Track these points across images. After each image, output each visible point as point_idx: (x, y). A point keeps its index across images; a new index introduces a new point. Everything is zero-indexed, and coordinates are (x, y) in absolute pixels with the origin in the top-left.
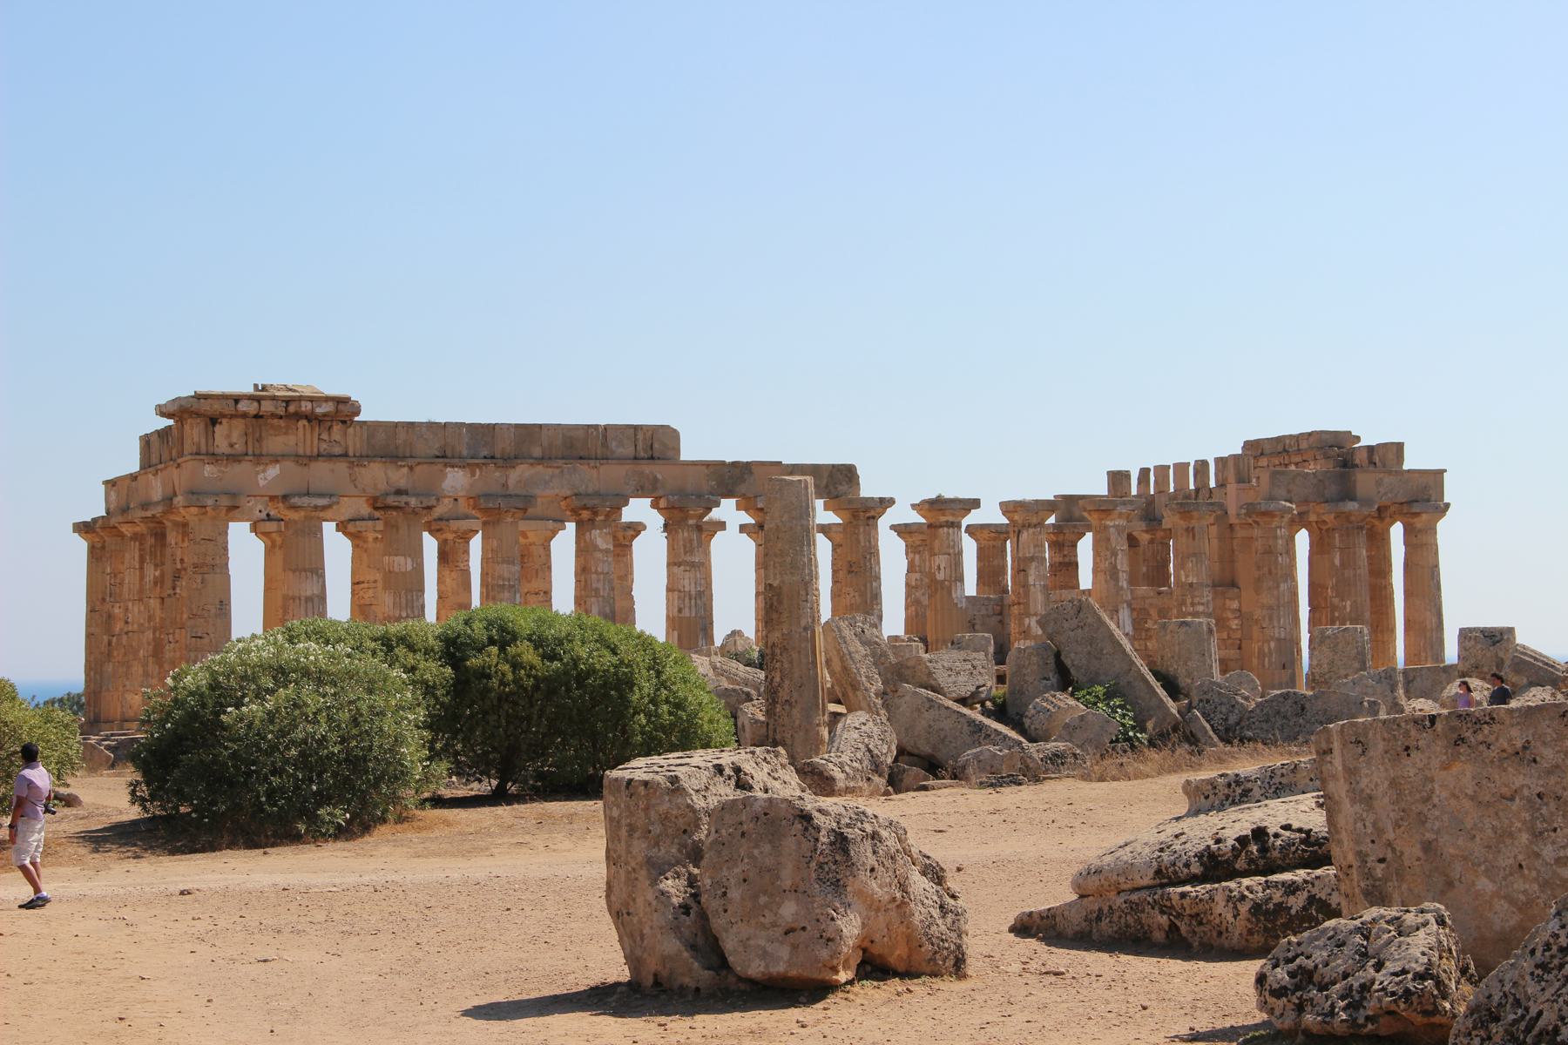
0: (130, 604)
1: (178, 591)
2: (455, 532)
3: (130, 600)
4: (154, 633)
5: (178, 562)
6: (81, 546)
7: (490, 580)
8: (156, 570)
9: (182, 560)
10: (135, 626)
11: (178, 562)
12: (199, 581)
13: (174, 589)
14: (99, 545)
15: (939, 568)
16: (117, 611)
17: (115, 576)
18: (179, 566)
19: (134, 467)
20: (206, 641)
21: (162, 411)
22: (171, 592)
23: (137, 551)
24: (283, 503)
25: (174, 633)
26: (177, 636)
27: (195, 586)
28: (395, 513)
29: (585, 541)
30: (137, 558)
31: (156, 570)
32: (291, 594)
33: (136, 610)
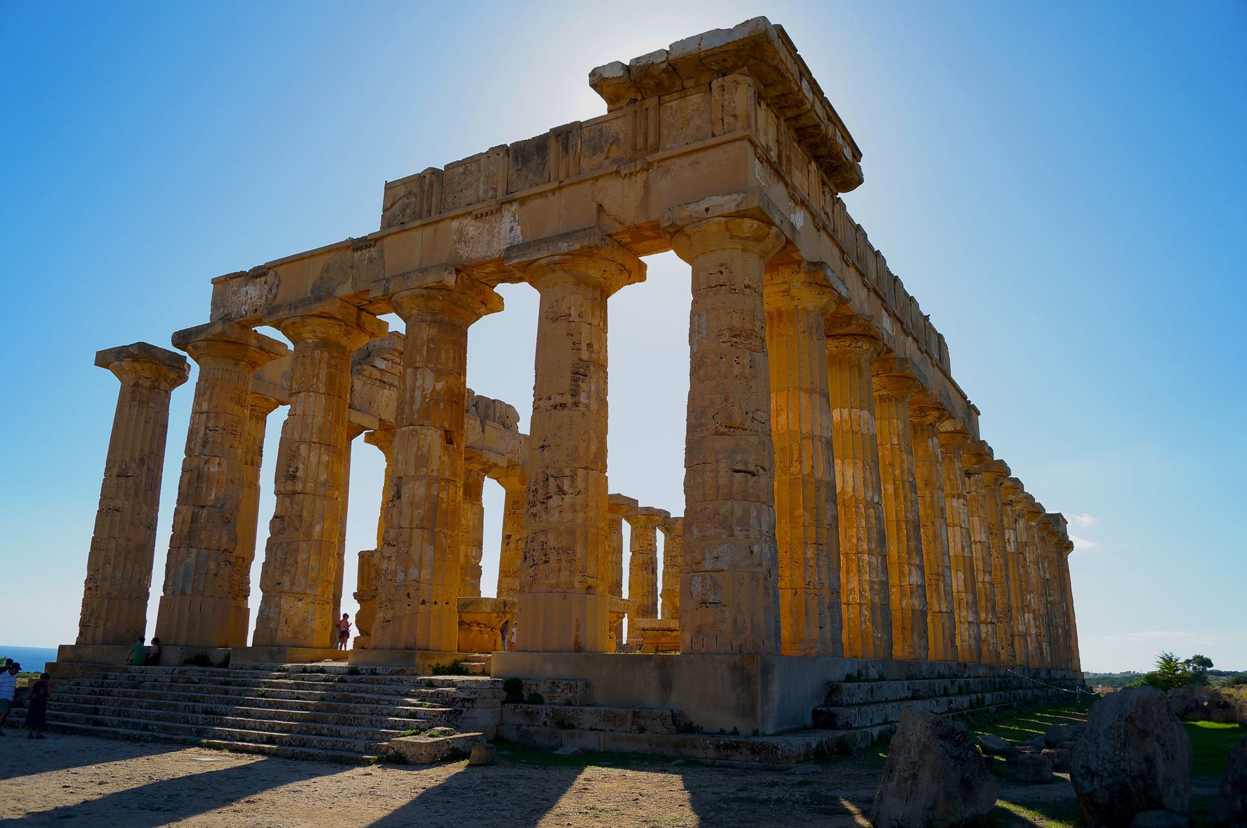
0: (303, 448)
1: (583, 398)
2: (485, 464)
3: (302, 441)
4: (428, 488)
5: (584, 346)
6: (109, 386)
7: (898, 472)
8: (437, 380)
9: (590, 345)
10: (310, 484)
11: (584, 346)
12: (746, 361)
13: (575, 393)
14: (148, 383)
15: (1009, 540)
16: (214, 469)
17: (217, 415)
18: (585, 355)
19: (368, 221)
20: (763, 480)
21: (599, 81)
22: (568, 399)
23: (324, 365)
24: (808, 272)
25: (573, 477)
26: (580, 484)
27: (736, 370)
28: (866, 346)
29: (926, 450)
30: (323, 376)
31: (437, 380)
32: (806, 428)
33: (313, 457)
